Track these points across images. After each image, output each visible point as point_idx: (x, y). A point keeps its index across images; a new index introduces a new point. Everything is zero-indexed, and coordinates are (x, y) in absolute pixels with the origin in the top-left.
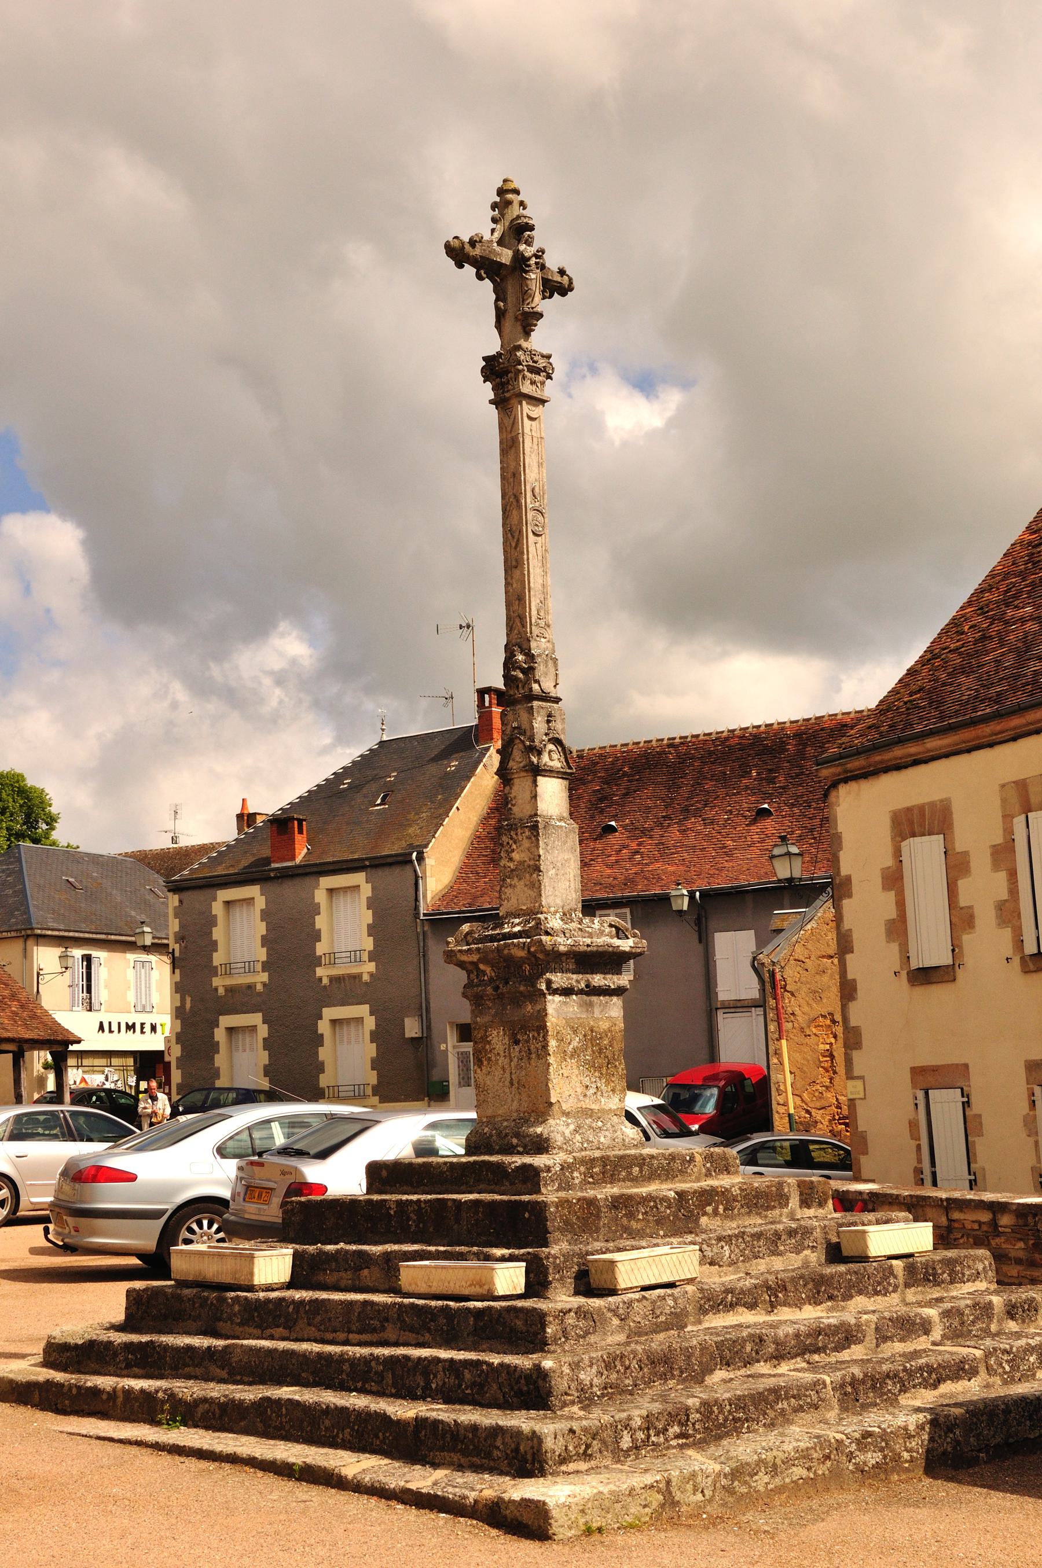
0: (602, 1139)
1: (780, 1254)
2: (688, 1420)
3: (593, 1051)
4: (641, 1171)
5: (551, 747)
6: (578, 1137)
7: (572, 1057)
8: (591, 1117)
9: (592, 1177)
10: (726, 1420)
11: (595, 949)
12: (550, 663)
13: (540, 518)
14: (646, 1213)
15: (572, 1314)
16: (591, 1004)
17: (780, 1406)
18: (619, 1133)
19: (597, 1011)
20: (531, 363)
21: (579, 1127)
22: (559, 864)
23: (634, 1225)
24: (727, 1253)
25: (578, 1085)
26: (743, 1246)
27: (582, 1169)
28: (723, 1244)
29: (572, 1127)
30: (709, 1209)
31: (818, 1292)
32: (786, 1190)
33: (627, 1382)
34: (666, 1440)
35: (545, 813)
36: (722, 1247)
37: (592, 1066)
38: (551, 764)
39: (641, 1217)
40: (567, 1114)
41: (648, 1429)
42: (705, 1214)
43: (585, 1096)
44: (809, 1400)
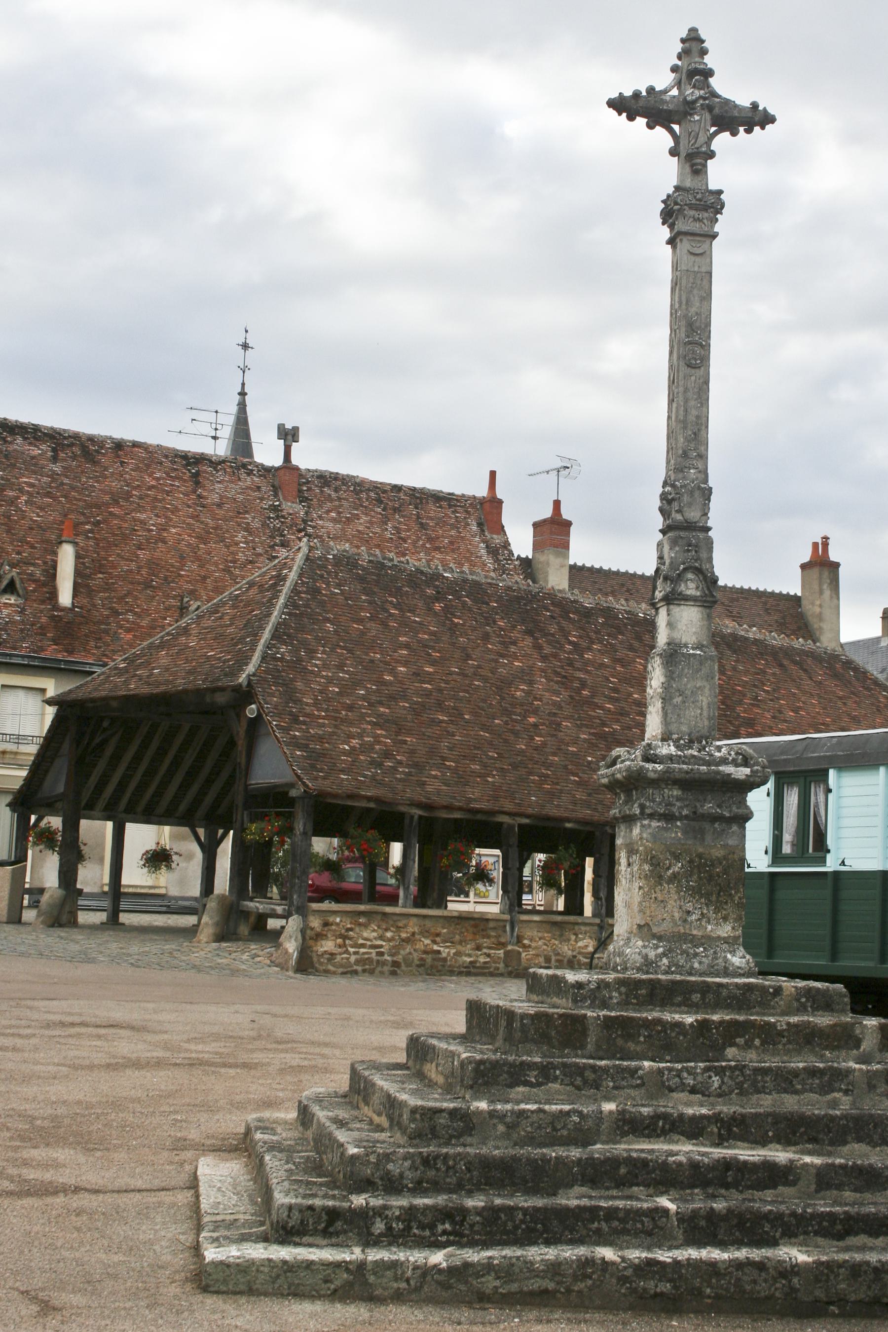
0: (696, 965)
1: (796, 1092)
2: (464, 1219)
3: (700, 878)
4: (703, 998)
5: (690, 576)
6: (665, 961)
7: (671, 880)
8: (691, 942)
9: (635, 998)
10: (516, 1227)
11: (697, 776)
12: (697, 494)
13: (698, 350)
14: (650, 1036)
15: (444, 1114)
16: (702, 832)
17: (596, 1225)
18: (721, 960)
19: (709, 838)
20: (694, 202)
21: (670, 950)
22: (688, 693)
23: (631, 1046)
24: (716, 1085)
25: (675, 910)
26: (741, 1078)
27: (623, 989)
28: (713, 1075)
29: (661, 950)
30: (740, 1041)
31: (794, 1133)
32: (858, 1032)
33: (448, 1180)
34: (433, 1234)
35: (677, 641)
36: (710, 1077)
37: (695, 892)
38: (689, 592)
39: (642, 1039)
40: (660, 938)
41: (410, 1221)
42: (732, 1045)
43: (685, 921)
44: (639, 1226)
